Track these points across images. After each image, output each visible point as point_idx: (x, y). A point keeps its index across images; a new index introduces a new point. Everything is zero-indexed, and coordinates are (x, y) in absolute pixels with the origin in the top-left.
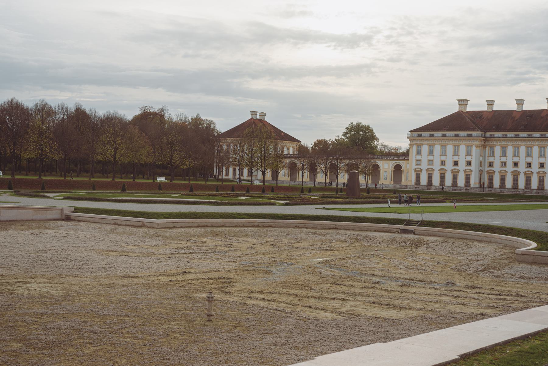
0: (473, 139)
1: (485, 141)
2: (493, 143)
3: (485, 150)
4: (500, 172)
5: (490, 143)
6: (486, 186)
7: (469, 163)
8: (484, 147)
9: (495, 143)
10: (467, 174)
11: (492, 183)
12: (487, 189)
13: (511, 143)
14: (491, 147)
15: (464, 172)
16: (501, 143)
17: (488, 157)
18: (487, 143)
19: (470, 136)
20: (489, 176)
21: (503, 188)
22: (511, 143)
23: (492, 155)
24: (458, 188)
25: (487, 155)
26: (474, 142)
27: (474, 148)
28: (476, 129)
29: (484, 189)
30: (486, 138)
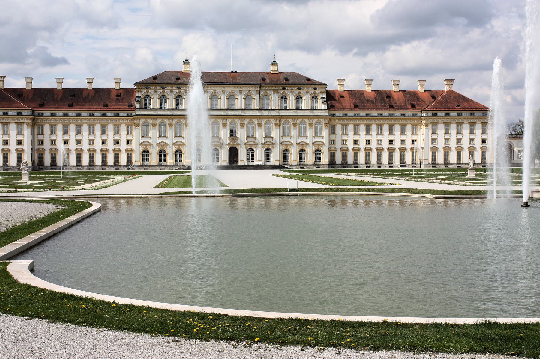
0: (23, 118)
1: (34, 119)
2: (42, 122)
3: (34, 128)
4: (50, 150)
5: (39, 121)
6: (36, 164)
7: (20, 142)
8: (33, 126)
9: (44, 122)
10: (19, 153)
11: (43, 161)
12: (38, 168)
13: (61, 122)
14: (39, 126)
15: (87, 151)
16: (50, 122)
17: (37, 135)
18: (35, 121)
19: (20, 114)
20: (39, 154)
21: (54, 166)
22: (61, 122)
23: (41, 133)
24: (10, 168)
25: (36, 133)
26: (25, 120)
27: (25, 126)
28: (25, 107)
29: (35, 167)
30: (35, 116)
